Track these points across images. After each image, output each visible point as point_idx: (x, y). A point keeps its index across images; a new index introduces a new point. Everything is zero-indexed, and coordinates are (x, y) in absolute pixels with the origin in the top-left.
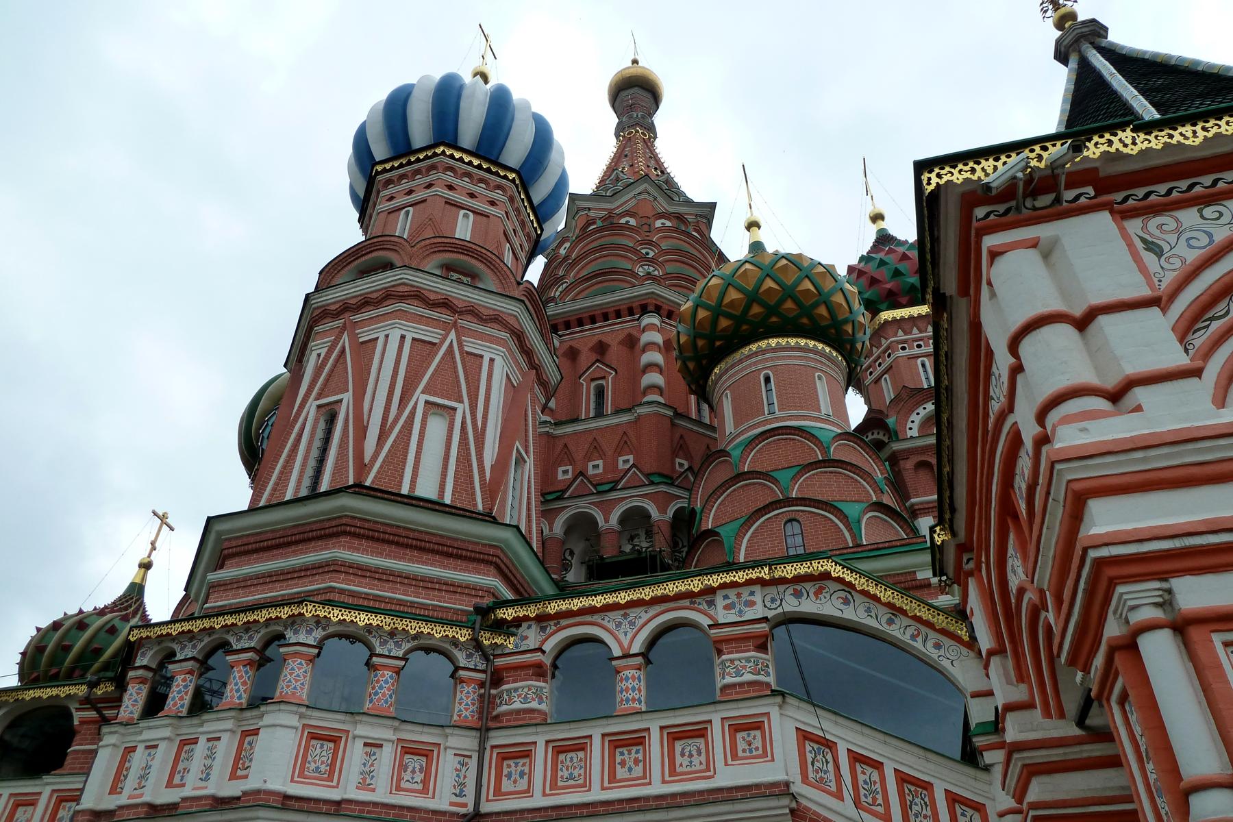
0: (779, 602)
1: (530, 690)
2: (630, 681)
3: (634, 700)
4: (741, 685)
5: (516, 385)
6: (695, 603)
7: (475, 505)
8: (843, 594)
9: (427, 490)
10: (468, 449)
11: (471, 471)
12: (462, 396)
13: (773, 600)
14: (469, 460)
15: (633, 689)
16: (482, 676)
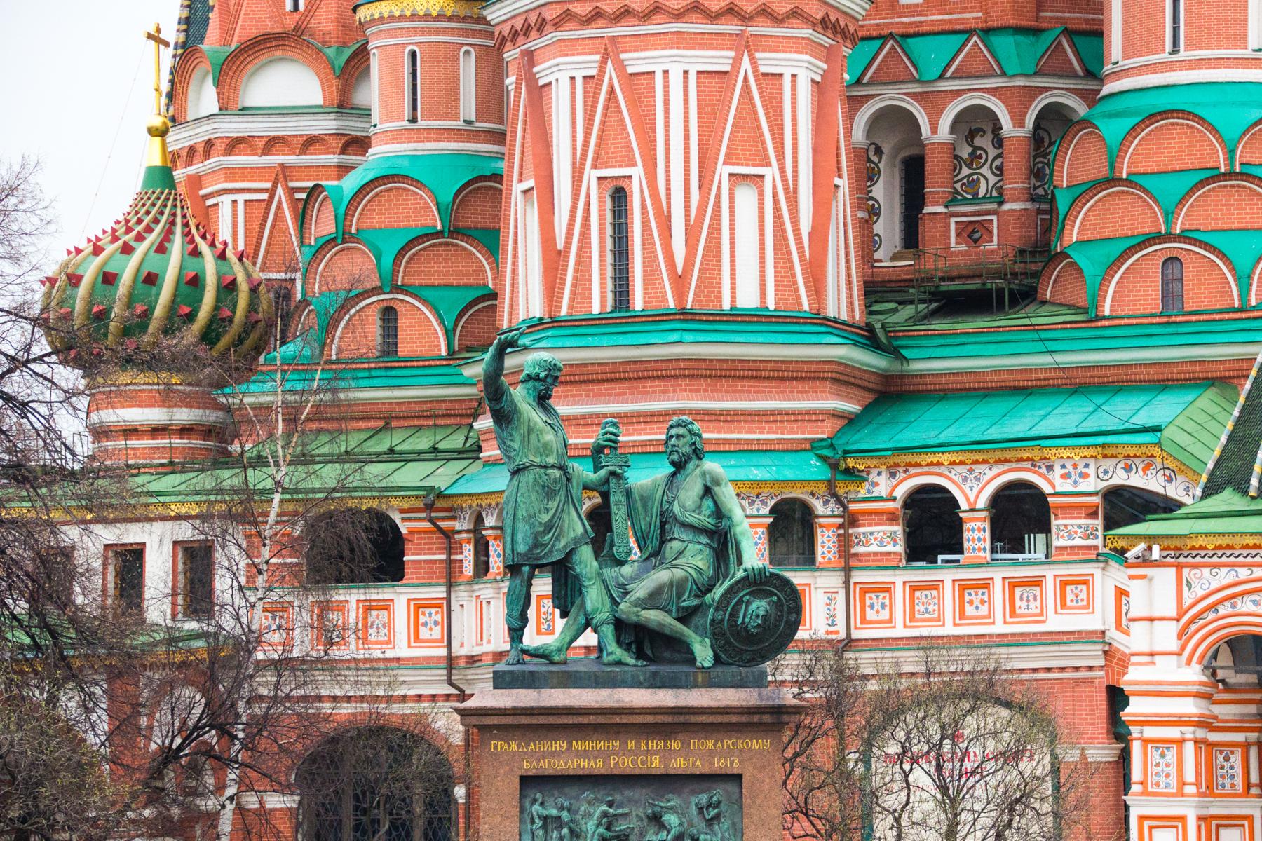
0: (1110, 474)
1: (885, 534)
2: (976, 532)
3: (979, 549)
4: (1072, 547)
5: (818, 79)
6: (1034, 466)
7: (800, 304)
8: (1167, 472)
9: (748, 299)
10: (784, 231)
11: (791, 261)
12: (767, 156)
13: (1106, 472)
14: (787, 246)
15: (979, 539)
16: (840, 520)
